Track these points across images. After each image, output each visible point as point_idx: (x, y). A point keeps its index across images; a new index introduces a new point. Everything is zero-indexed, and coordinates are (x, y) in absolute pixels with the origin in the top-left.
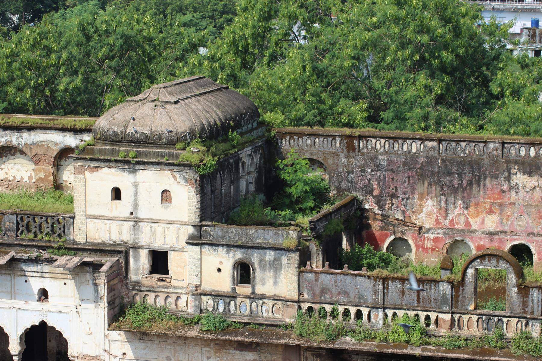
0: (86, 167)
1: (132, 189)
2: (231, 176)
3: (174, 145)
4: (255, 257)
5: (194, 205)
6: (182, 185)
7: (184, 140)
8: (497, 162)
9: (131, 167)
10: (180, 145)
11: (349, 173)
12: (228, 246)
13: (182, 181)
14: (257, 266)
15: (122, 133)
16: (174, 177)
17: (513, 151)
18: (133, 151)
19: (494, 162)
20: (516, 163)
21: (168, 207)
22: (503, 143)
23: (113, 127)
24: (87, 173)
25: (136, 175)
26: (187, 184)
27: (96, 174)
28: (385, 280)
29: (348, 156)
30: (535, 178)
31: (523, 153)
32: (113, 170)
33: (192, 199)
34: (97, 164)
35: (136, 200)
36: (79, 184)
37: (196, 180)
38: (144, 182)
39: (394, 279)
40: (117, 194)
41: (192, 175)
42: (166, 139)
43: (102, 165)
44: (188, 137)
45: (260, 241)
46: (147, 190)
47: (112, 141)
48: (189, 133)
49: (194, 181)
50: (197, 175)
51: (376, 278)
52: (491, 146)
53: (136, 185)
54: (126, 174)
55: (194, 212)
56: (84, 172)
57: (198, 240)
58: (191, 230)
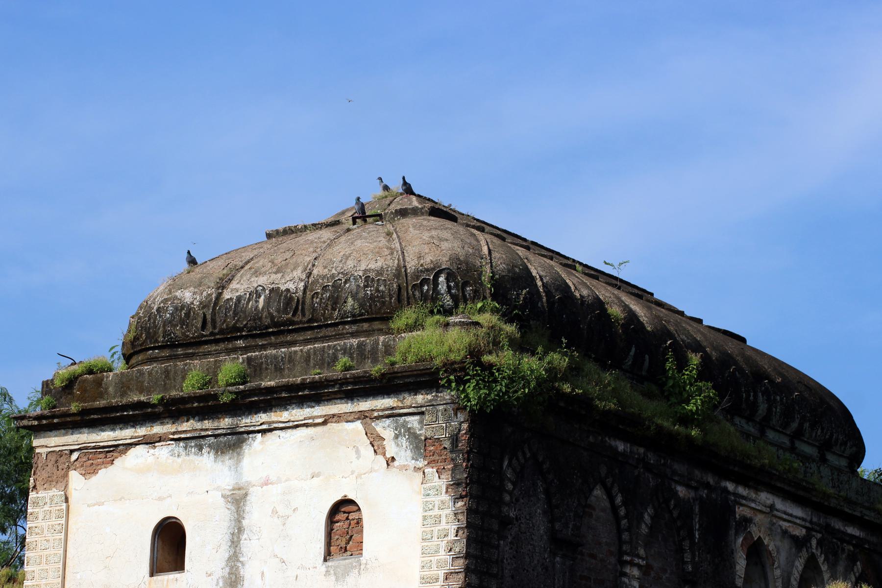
0: (75, 456)
1: (223, 515)
2: (680, 550)
3: (386, 319)
5: (443, 544)
6: (405, 468)
7: (424, 297)
9: (226, 422)
10: (408, 315)
15: (204, 305)
16: (376, 442)
21: (346, 572)
23: (178, 294)
24: (75, 477)
25: (239, 461)
26: (421, 463)
27: (105, 474)
32: (163, 451)
33: (438, 520)
34: (106, 436)
35: (234, 559)
36: (45, 524)
37: (455, 439)
38: (267, 483)
41: (436, 416)
42: (354, 297)
43: (126, 434)
44: (442, 287)
46: (275, 512)
47: (172, 345)
48: (450, 277)
49: (447, 444)
50: (461, 417)
53: (238, 500)
54: (206, 460)
55: (441, 574)
56: (66, 476)
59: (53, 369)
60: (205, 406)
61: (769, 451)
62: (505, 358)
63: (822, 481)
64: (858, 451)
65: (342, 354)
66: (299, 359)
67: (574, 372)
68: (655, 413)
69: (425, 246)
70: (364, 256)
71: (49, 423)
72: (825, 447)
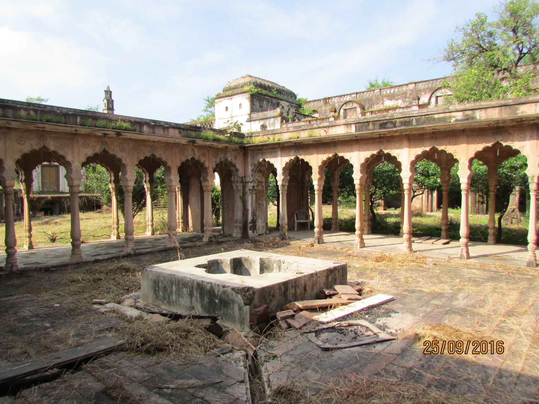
4: (267, 122)
8: (378, 97)
11: (326, 112)
12: (259, 120)
13: (245, 98)
14: (268, 126)
17: (384, 92)
18: (230, 92)
19: (377, 98)
20: (385, 96)
22: (381, 89)
28: (310, 121)
29: (325, 107)
30: (393, 101)
31: (388, 92)
39: (313, 120)
40: (227, 108)
41: (247, 95)
45: (269, 116)
51: (306, 121)
52: (376, 91)
57: (250, 120)
58: (248, 117)
59: (216, 94)
60: (229, 96)
61: (285, 97)
62: (253, 90)
63: (291, 100)
64: (296, 98)
65: (239, 90)
66: (236, 91)
67: (261, 90)
68: (271, 94)
69: (248, 80)
70: (242, 81)
71: (216, 99)
72: (291, 97)
